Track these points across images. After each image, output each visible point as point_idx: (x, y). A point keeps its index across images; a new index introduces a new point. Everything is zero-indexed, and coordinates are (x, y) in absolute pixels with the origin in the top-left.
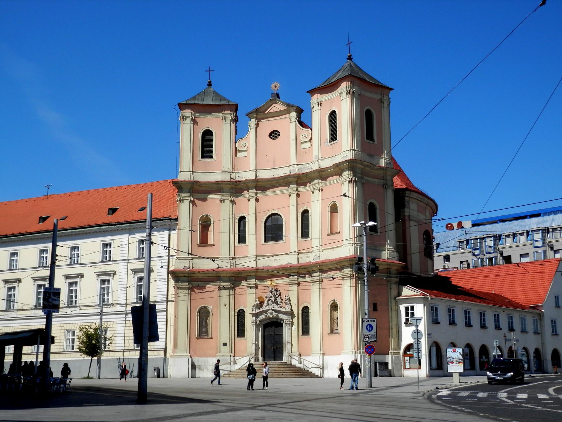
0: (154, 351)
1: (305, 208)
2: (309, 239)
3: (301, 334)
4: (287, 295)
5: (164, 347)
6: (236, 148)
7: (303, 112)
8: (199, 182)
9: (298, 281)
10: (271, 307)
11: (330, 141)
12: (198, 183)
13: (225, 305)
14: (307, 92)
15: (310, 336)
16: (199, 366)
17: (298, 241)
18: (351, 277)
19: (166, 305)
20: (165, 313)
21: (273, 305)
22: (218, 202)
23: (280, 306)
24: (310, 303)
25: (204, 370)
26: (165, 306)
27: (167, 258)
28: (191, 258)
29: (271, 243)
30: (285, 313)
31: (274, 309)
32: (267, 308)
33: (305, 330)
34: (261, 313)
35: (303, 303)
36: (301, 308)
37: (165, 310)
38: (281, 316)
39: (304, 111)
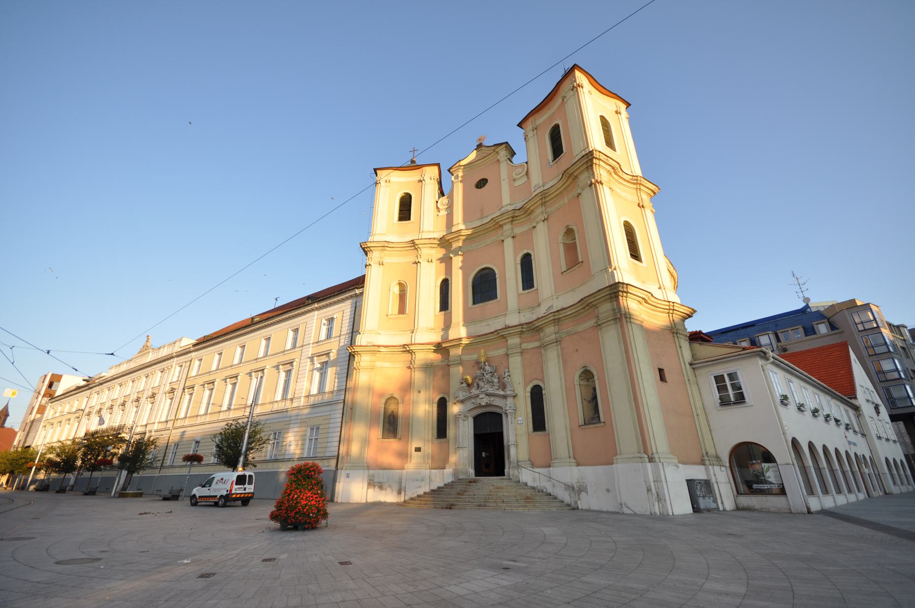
0: (324, 459)
1: (525, 252)
2: (534, 289)
3: (532, 431)
4: (507, 370)
6: (438, 208)
7: (515, 156)
9: (520, 347)
10: (483, 390)
11: (553, 161)
14: (517, 125)
15: (547, 432)
16: (380, 483)
17: (519, 295)
18: (614, 319)
21: (486, 386)
23: (496, 387)
24: (543, 381)
25: (387, 489)
29: (481, 304)
30: (505, 397)
31: (487, 392)
32: (477, 392)
33: (539, 422)
34: (470, 398)
35: (531, 381)
36: (529, 389)
38: (497, 402)
39: (515, 154)
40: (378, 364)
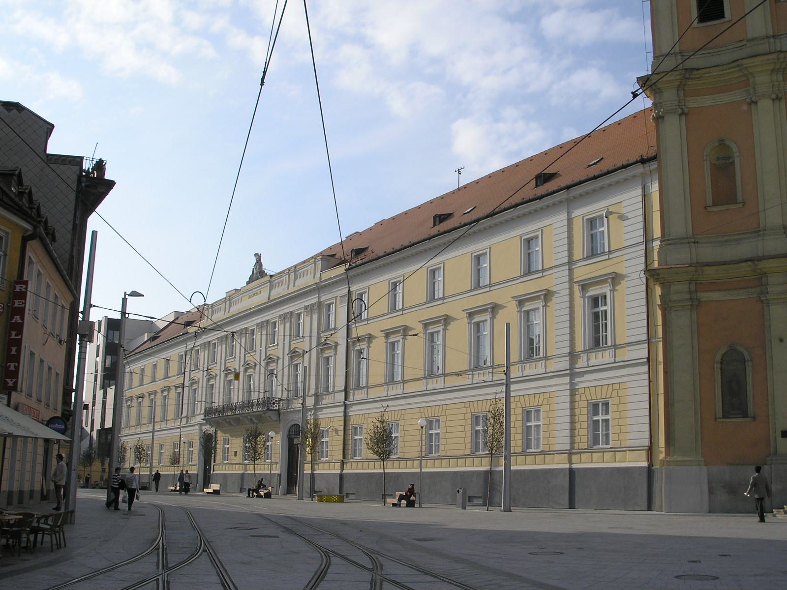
5: (646, 443)
8: (695, 69)
12: (695, 72)
13: (781, 340)
19: (646, 350)
20: (646, 368)
22: (745, 107)
26: (644, 353)
27: (643, 247)
28: (693, 240)
37: (646, 360)
40: (704, 296)
